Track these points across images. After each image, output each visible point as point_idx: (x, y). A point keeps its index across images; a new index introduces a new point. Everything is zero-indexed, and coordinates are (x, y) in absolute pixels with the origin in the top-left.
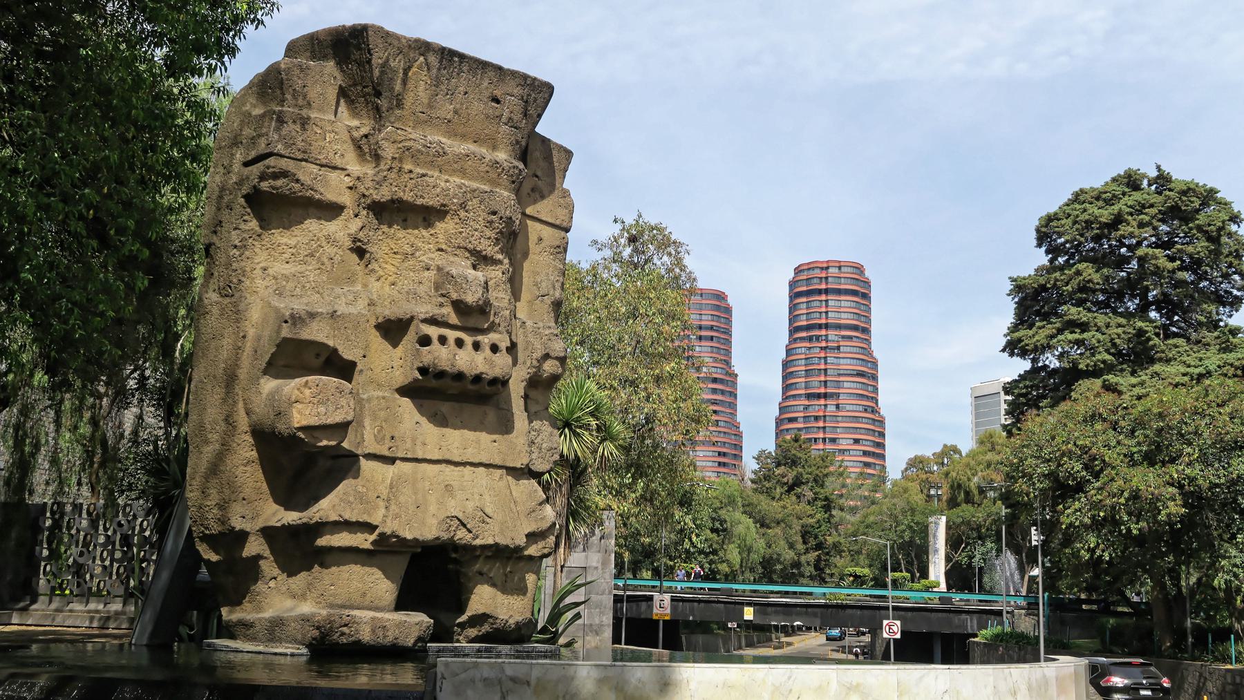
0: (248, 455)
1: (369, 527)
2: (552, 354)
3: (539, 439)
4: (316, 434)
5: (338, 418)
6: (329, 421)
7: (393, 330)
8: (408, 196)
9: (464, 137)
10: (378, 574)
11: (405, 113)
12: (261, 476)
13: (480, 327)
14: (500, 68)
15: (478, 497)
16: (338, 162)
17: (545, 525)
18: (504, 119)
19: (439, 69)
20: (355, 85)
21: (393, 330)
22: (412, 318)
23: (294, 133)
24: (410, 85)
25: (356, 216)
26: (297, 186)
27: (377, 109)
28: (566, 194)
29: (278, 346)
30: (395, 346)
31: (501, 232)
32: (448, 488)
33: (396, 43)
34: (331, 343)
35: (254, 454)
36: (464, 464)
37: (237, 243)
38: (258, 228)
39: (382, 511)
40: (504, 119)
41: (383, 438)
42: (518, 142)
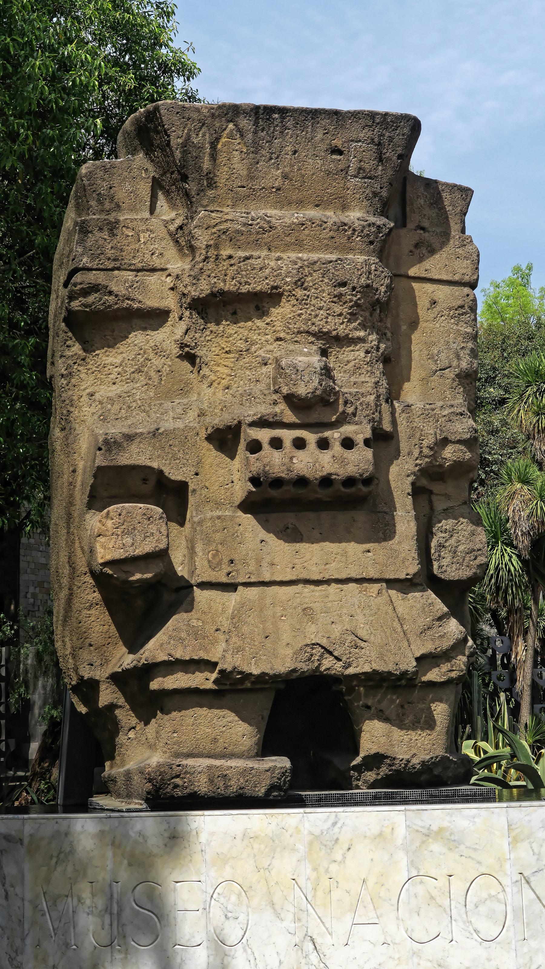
0: (90, 597)
1: (211, 665)
2: (452, 438)
3: (452, 541)
4: (126, 568)
5: (147, 547)
6: (138, 552)
7: (225, 439)
8: (230, 286)
9: (300, 204)
10: (231, 716)
11: (220, 192)
12: (108, 618)
13: (326, 420)
14: (336, 113)
15: (347, 619)
16: (157, 262)
17: (446, 644)
18: (352, 171)
19: (255, 133)
20: (164, 173)
21: (225, 439)
22: (240, 422)
23: (101, 242)
24: (222, 158)
25: (181, 319)
26: (111, 299)
27: (187, 194)
28: (466, 242)
29: (95, 476)
30: (232, 457)
31: (357, 305)
32: (308, 612)
33: (195, 115)
34: (155, 465)
35: (97, 595)
36: (328, 582)
37: (63, 371)
38: (81, 352)
39: (224, 645)
40: (352, 171)
41: (220, 563)
42: (375, 194)
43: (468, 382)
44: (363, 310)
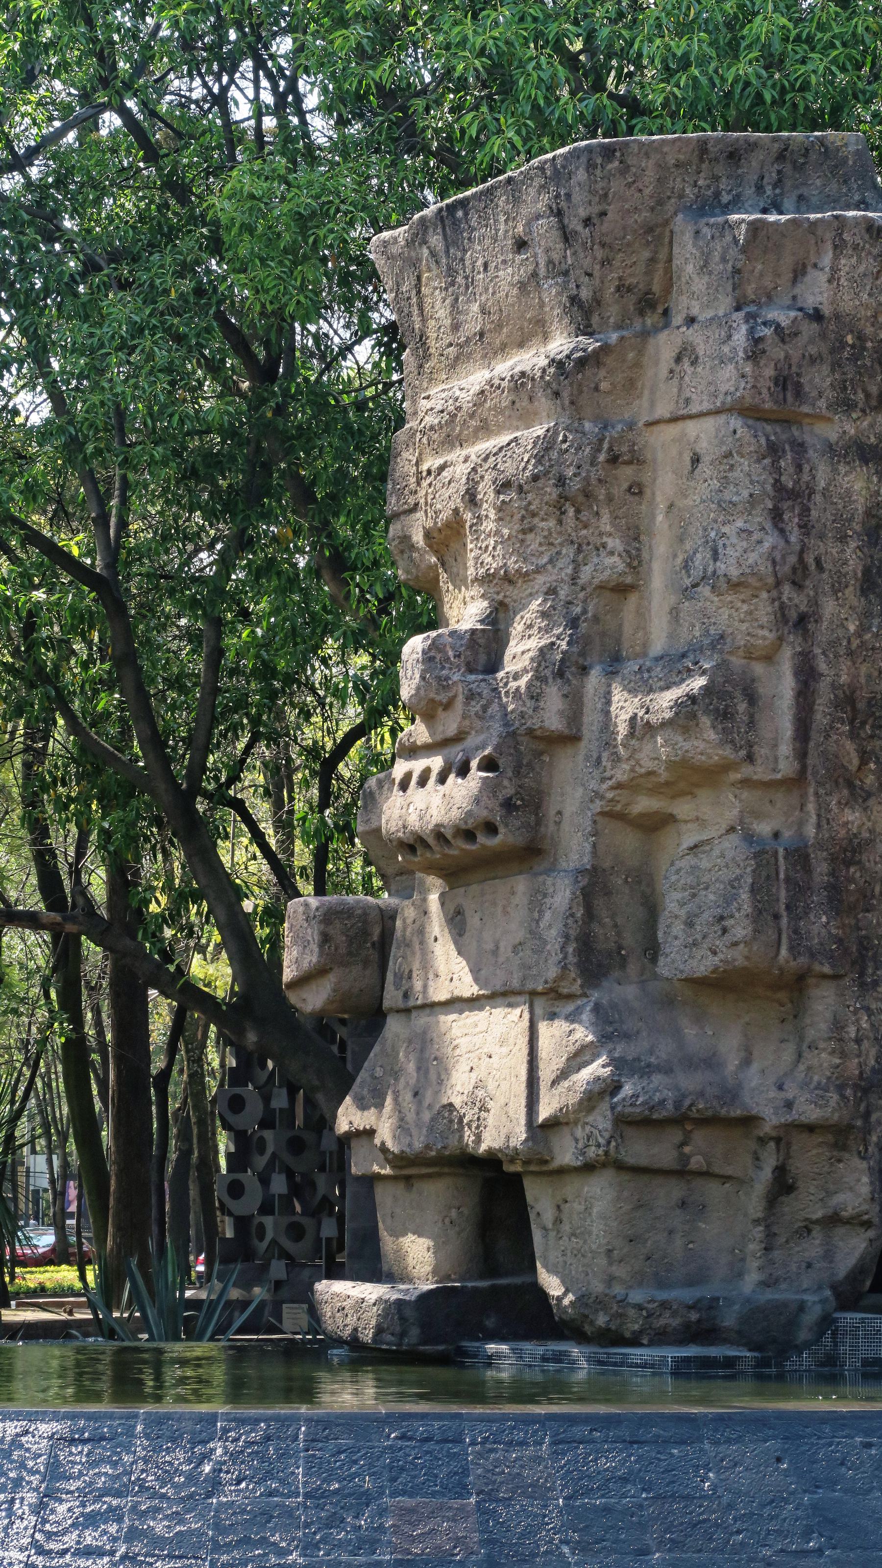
9: (503, 349)
18: (542, 271)
40: (542, 271)
43: (742, 597)
44: (543, 520)
